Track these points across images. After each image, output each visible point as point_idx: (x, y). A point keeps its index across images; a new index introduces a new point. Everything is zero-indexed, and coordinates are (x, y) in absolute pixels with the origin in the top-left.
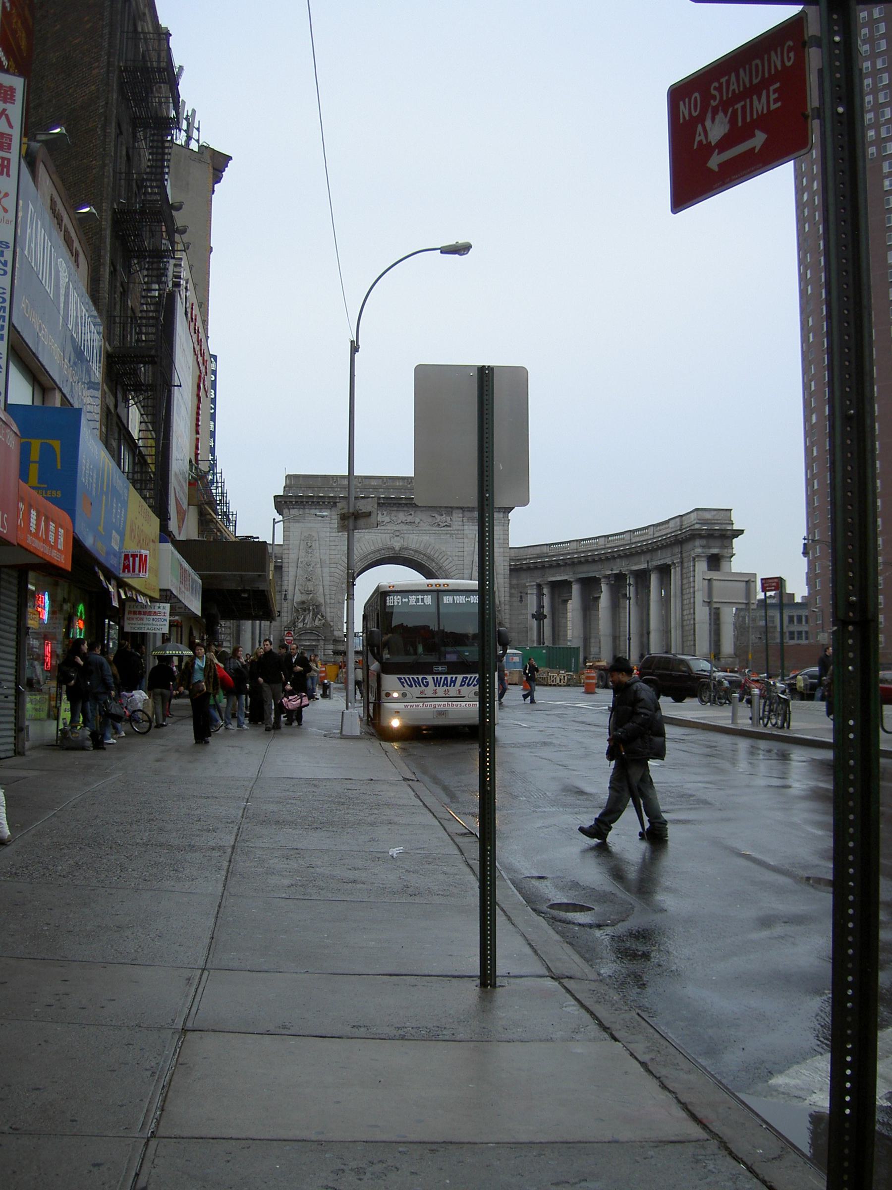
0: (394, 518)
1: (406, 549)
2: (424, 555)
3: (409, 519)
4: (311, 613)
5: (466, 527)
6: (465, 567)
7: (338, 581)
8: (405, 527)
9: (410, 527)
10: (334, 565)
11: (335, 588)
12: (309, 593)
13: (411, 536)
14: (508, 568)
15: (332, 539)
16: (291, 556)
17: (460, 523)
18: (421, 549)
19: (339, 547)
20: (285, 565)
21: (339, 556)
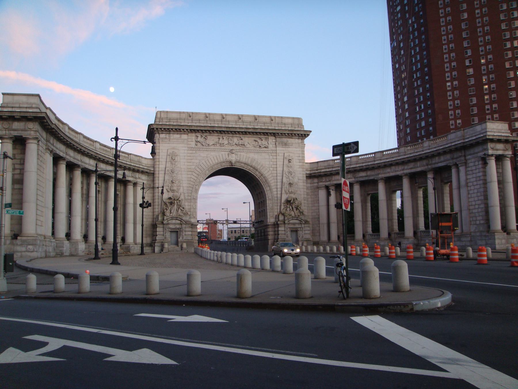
0: (229, 142)
1: (239, 162)
2: (251, 166)
3: (241, 142)
4: (176, 206)
5: (278, 148)
6: (278, 175)
7: (193, 184)
8: (238, 148)
9: (241, 148)
10: (190, 173)
11: (191, 189)
12: (173, 191)
13: (242, 153)
14: (305, 176)
15: (189, 155)
16: (160, 166)
17: (274, 146)
18: (249, 162)
19: (193, 161)
20: (157, 172)
21: (193, 167)
